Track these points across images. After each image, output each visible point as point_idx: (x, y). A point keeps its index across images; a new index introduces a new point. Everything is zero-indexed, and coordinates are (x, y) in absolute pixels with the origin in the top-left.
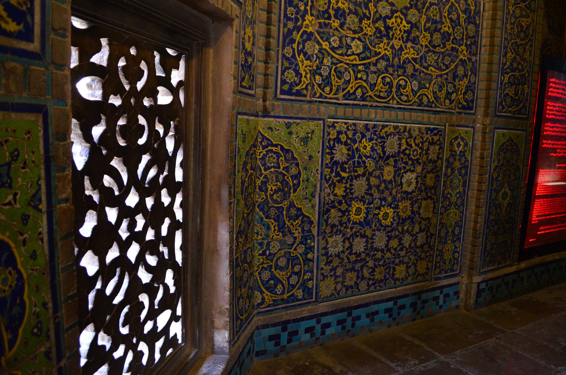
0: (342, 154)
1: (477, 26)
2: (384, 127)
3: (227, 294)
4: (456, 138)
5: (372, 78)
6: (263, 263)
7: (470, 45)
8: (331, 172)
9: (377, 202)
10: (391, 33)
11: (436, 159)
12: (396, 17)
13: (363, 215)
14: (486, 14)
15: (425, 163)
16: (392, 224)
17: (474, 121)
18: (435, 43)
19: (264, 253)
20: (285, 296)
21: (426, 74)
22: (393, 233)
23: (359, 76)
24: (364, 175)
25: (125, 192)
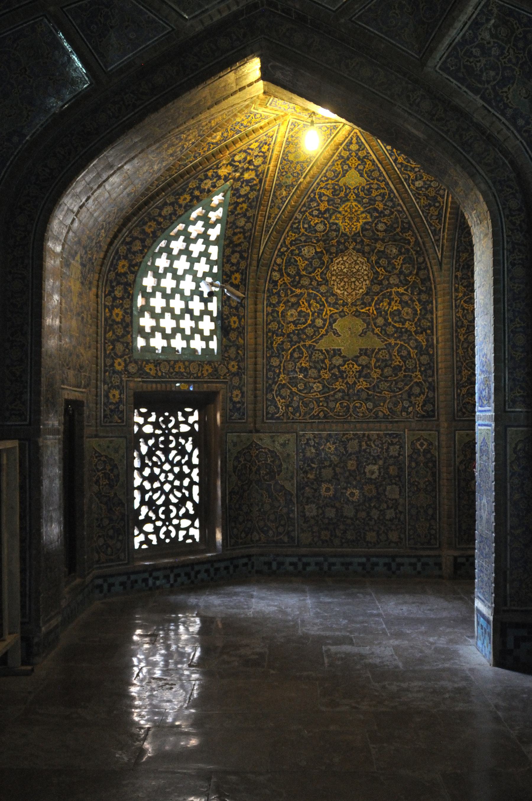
0: (312, 453)
1: (431, 356)
2: (344, 435)
3: (221, 520)
4: (418, 440)
5: (332, 405)
6: (259, 516)
7: (425, 370)
8: (304, 463)
9: (343, 484)
10: (345, 375)
11: (397, 455)
12: (348, 364)
13: (331, 493)
14: (440, 345)
15: (386, 459)
16: (359, 501)
17: (438, 425)
18: (386, 374)
19: (260, 510)
20: (275, 539)
21: (379, 397)
22: (361, 507)
23: (321, 404)
24: (330, 466)
25: (163, 464)
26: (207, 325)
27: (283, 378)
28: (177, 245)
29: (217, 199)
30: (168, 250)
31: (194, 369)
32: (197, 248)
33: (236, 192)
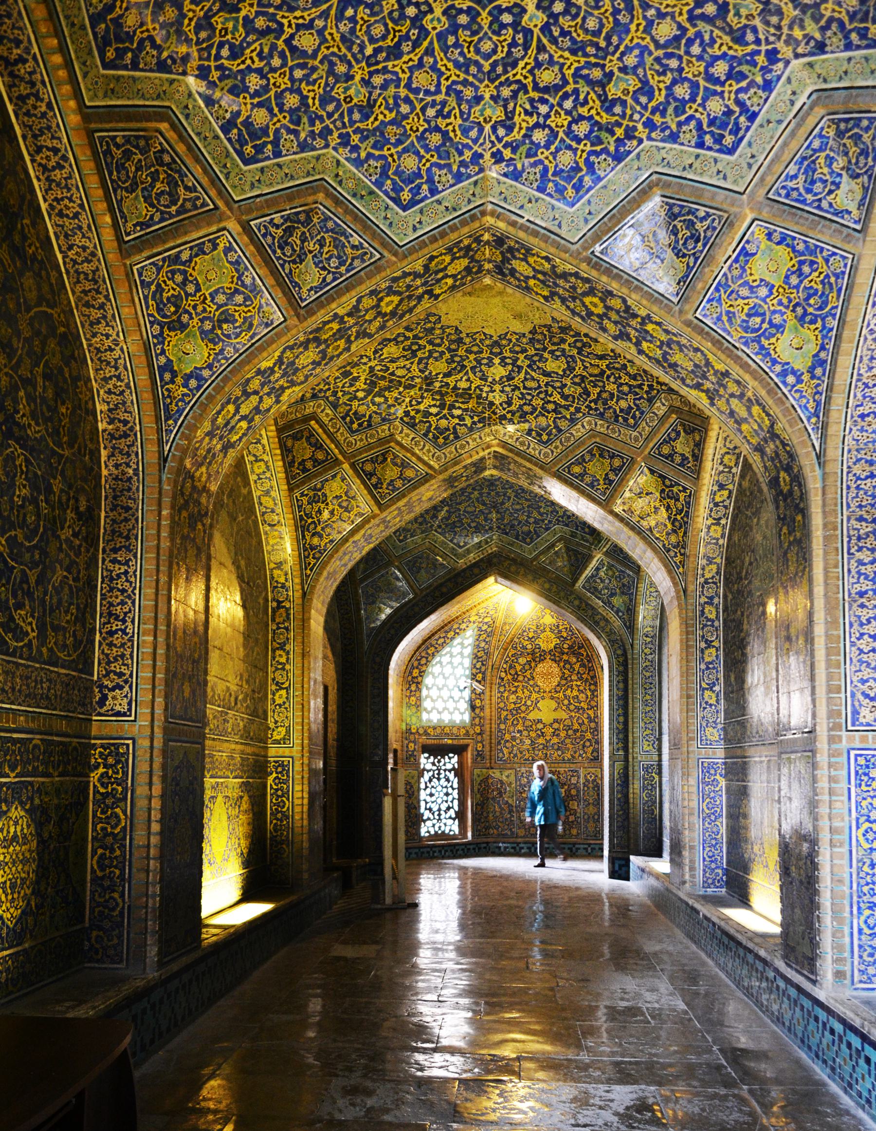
26: (464, 706)
27: (507, 737)
28: (445, 659)
29: (469, 633)
30: (440, 662)
31: (455, 731)
32: (457, 660)
33: (480, 629)
